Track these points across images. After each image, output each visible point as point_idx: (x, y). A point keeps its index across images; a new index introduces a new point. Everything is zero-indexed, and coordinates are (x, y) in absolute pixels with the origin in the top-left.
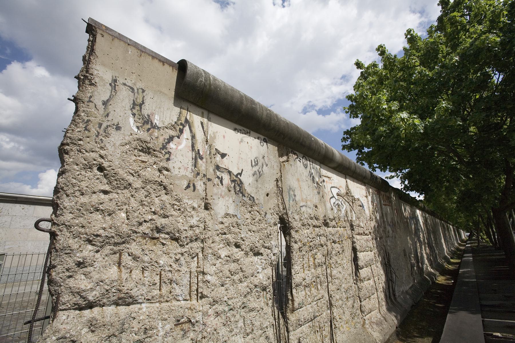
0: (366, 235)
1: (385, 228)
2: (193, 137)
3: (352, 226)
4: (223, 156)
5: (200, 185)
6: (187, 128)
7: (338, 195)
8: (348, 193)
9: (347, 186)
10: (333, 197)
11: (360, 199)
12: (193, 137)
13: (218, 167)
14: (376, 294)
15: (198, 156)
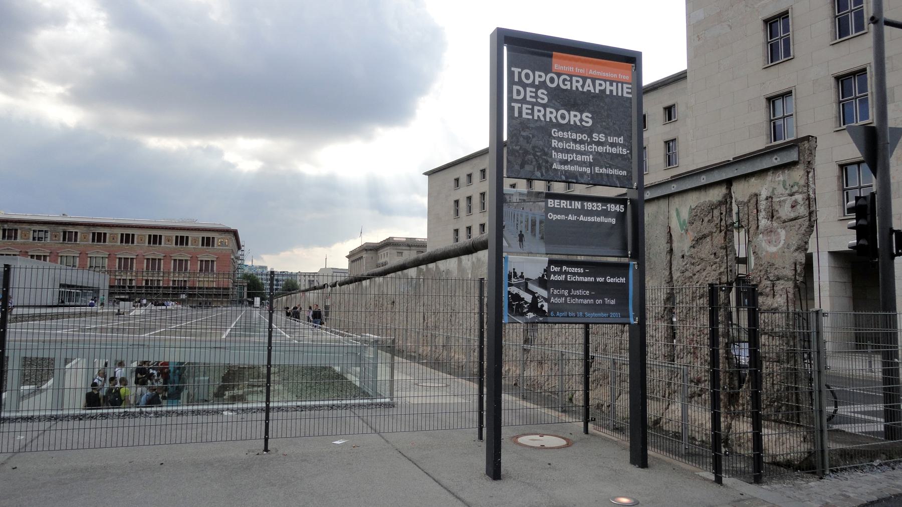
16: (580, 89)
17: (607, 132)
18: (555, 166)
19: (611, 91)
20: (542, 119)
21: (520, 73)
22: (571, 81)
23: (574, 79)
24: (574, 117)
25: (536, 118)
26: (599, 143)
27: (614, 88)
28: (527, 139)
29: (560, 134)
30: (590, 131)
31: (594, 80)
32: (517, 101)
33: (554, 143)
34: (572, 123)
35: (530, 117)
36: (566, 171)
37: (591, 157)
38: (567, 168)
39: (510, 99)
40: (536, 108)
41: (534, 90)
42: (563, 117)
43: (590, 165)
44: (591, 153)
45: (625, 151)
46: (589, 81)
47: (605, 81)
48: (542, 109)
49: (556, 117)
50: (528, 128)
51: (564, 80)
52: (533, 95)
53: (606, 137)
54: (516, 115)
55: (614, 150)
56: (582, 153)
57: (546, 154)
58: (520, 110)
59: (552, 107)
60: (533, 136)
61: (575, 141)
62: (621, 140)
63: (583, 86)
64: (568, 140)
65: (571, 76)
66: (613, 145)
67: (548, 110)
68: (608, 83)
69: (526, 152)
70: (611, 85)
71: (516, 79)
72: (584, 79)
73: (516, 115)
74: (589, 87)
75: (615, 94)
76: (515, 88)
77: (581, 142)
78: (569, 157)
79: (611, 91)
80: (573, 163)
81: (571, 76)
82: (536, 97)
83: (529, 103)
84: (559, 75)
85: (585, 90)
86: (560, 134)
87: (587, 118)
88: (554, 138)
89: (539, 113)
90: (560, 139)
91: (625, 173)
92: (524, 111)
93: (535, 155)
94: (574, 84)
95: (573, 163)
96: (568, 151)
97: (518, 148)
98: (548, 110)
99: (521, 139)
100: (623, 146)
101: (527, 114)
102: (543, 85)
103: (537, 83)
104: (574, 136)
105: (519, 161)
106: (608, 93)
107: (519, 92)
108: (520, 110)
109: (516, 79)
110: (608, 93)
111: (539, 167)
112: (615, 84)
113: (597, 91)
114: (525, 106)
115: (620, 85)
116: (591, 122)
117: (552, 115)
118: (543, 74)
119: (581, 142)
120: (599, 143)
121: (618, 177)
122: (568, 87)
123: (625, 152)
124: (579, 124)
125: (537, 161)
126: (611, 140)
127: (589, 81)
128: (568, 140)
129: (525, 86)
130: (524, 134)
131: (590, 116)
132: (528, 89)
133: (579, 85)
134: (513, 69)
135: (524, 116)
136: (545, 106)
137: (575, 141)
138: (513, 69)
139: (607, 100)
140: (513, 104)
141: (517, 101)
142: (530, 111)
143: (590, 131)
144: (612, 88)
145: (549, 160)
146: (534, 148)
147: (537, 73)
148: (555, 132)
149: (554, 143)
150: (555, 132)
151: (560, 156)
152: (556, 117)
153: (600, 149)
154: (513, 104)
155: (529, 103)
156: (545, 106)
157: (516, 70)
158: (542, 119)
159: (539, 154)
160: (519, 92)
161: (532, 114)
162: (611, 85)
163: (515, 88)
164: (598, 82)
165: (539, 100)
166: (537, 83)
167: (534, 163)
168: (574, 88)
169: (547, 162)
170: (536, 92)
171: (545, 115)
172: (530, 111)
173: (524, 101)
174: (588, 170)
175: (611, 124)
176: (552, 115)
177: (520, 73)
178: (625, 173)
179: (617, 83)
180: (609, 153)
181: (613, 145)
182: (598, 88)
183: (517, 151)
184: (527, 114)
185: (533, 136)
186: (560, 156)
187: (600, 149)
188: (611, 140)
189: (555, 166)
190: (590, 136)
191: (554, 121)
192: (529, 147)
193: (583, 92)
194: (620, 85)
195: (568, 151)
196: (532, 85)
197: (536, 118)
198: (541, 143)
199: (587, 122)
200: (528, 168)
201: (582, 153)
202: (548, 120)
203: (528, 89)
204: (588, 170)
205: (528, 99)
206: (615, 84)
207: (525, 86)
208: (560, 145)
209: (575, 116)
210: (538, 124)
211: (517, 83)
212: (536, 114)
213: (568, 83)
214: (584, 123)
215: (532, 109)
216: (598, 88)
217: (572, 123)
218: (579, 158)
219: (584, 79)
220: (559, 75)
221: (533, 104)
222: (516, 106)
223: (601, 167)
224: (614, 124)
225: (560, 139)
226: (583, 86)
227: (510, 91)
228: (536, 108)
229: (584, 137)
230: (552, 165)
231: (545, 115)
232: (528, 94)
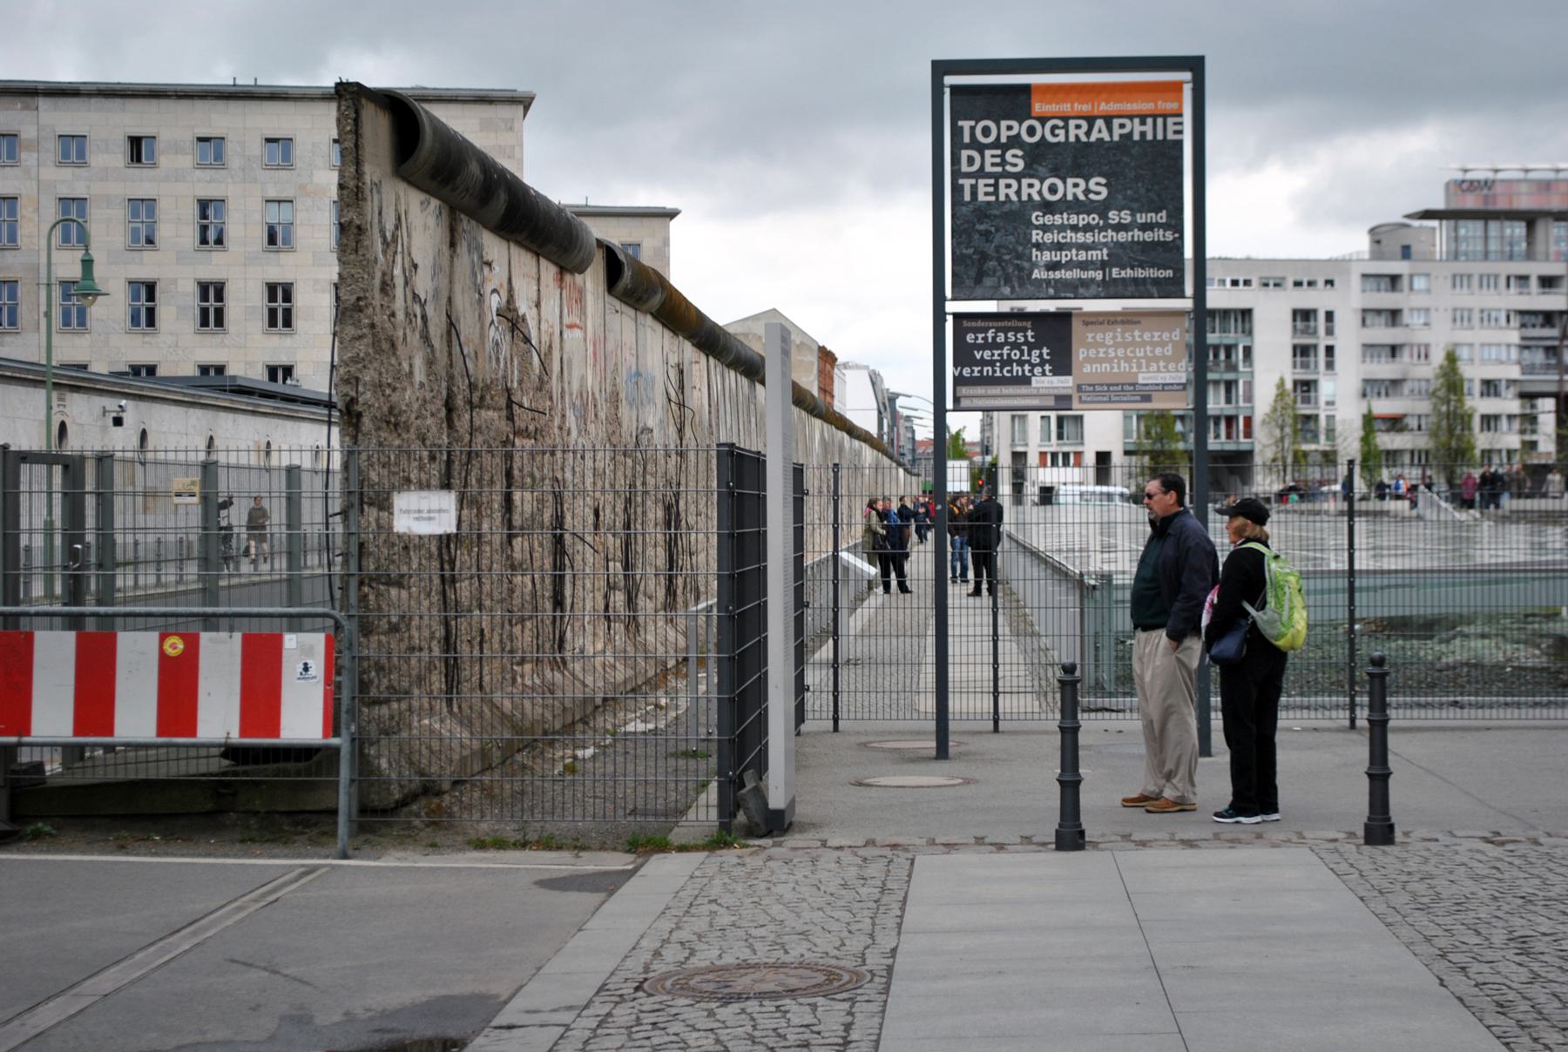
16: (1084, 139)
17: (1135, 205)
18: (1036, 274)
19: (1143, 134)
20: (1014, 198)
21: (973, 129)
22: (1066, 128)
23: (1072, 123)
24: (1072, 188)
25: (1002, 198)
26: (1119, 227)
27: (1148, 128)
28: (986, 235)
29: (1048, 220)
30: (1102, 209)
31: (1108, 119)
32: (968, 175)
33: (1036, 236)
34: (1070, 197)
35: (992, 198)
36: (1056, 281)
37: (1105, 251)
38: (1058, 275)
39: (956, 174)
40: (1002, 182)
41: (999, 152)
42: (1053, 190)
43: (1103, 265)
44: (1105, 244)
45: (1169, 236)
46: (1100, 123)
47: (1131, 117)
48: (1014, 182)
49: (1040, 193)
50: (987, 216)
51: (1054, 128)
52: (998, 160)
53: (1133, 215)
54: (967, 197)
55: (1148, 236)
56: (1086, 247)
57: (1019, 256)
58: (974, 189)
59: (1031, 176)
60: (997, 230)
61: (1075, 228)
62: (1162, 217)
63: (1088, 134)
64: (1062, 228)
65: (1065, 119)
66: (1145, 227)
67: (1025, 182)
68: (1137, 121)
70: (1143, 123)
71: (967, 139)
72: (1091, 120)
73: (967, 197)
74: (1100, 132)
75: (1150, 137)
76: (965, 154)
77: (1088, 228)
78: (1064, 257)
79: (1143, 134)
80: (1070, 265)
81: (1065, 119)
82: (1003, 163)
83: (989, 175)
84: (1043, 120)
85: (1093, 138)
86: (1048, 220)
87: (1098, 188)
88: (1037, 227)
89: (1007, 190)
90: (1045, 228)
91: (1169, 273)
92: (981, 190)
93: (999, 260)
94: (1072, 132)
95: (1070, 265)
96: (1059, 247)
97: (971, 251)
98: (1025, 182)
99: (976, 236)
100: (1165, 227)
101: (986, 194)
102: (1015, 141)
103: (1003, 140)
104: (1074, 220)
105: (973, 272)
106: (1136, 137)
107: (971, 160)
108: (974, 189)
109: (967, 139)
110: (1136, 137)
111: (1008, 280)
112: (1150, 121)
113: (1116, 138)
114: (982, 182)
115: (1160, 121)
116: (1104, 192)
117: (1034, 189)
118: (1014, 124)
119: (1088, 228)
120: (1119, 227)
122: (1062, 138)
123: (1169, 236)
124: (1082, 197)
125: (1003, 269)
126: (1141, 218)
127: (1100, 123)
128: (1062, 228)
130: (982, 227)
131: (1103, 181)
132: (988, 153)
133: (1081, 133)
134: (960, 123)
135: (981, 198)
136: (1018, 177)
137: (1075, 228)
138: (960, 123)
139: (1134, 151)
140: (961, 181)
141: (968, 175)
142: (991, 189)
143: (1102, 209)
144: (1143, 128)
145: (1026, 265)
146: (997, 249)
147: (1004, 124)
148: (1036, 217)
149: (1036, 236)
150: (1036, 217)
151: (1047, 256)
152: (1040, 193)
153: (1122, 237)
154: (961, 181)
155: (989, 175)
156: (1018, 177)
157: (966, 125)
158: (1014, 198)
159: (1007, 257)
160: (971, 160)
161: (996, 193)
162: (1143, 123)
163: (965, 154)
164: (1116, 122)
165: (1008, 168)
166: (1003, 140)
167: (999, 273)
168: (1072, 139)
169: (1020, 269)
170: (1002, 156)
171: (1018, 193)
172: (991, 189)
173: (981, 173)
174: (1099, 275)
175: (1142, 191)
176: (1034, 189)
177: (973, 129)
178: (1169, 273)
179: (1155, 117)
180: (1138, 243)
181: (1145, 227)
182: (1117, 132)
183: (970, 257)
184: (986, 194)
185: (997, 230)
186: (1047, 256)
187: (1122, 237)
188: (1141, 218)
189: (1036, 274)
190: (1103, 216)
191: (1036, 197)
193: (1088, 144)
194: (1160, 121)
195: (1059, 247)
196: (997, 144)
197: (1002, 198)
198: (1012, 239)
199: (1098, 193)
201: (1086, 247)
202: (1024, 198)
203: (988, 153)
204: (1099, 275)
205: (988, 169)
206: (1150, 121)
207: (981, 148)
208: (1048, 238)
209: (1076, 185)
210: (1007, 208)
211: (967, 147)
212: (1002, 191)
213: (1061, 132)
214: (1092, 196)
215: (996, 186)
216: (1117, 132)
217: (1070, 197)
218: (1082, 256)
219: (1091, 120)
220: (1043, 120)
221: (997, 177)
222: (967, 183)
223: (1123, 268)
224: (1148, 190)
225: (1045, 228)
226: (1088, 134)
227: (955, 160)
228: (1002, 182)
229: (1094, 219)
230: (1031, 273)
231: (1018, 193)
232: (989, 160)
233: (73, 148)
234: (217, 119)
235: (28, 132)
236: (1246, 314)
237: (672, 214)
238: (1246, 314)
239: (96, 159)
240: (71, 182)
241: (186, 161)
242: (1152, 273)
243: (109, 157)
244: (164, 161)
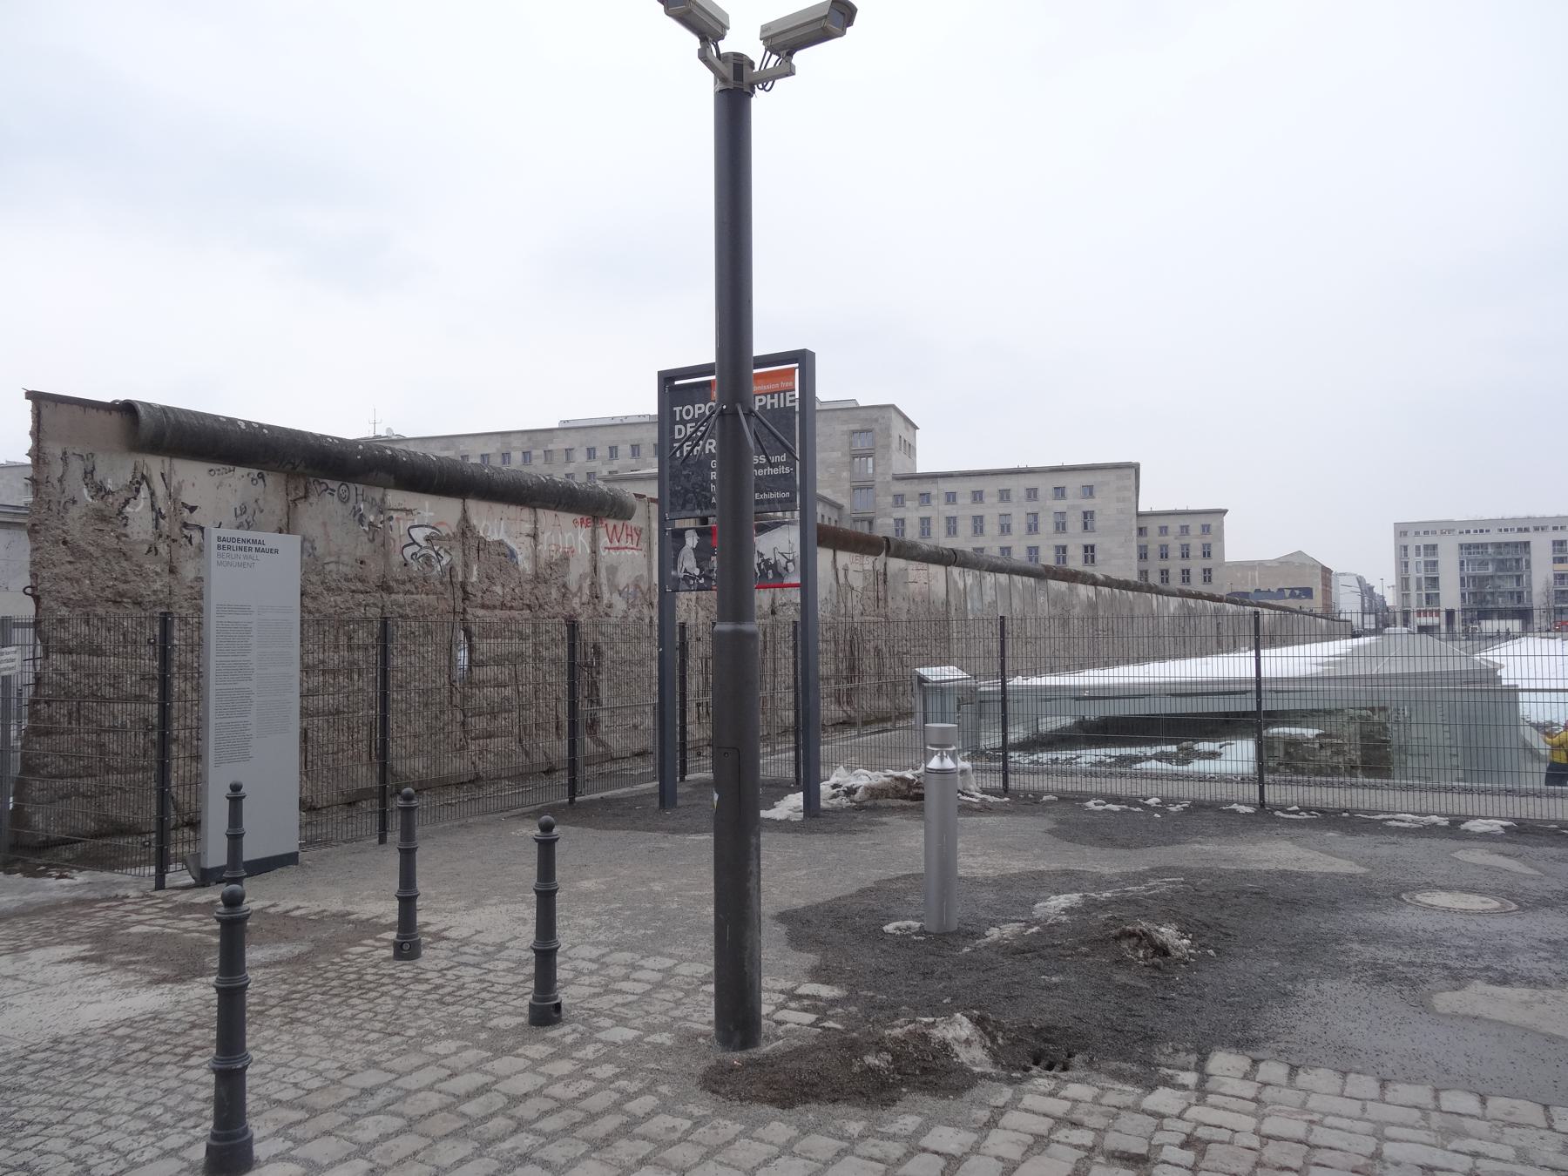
0: (511, 608)
1: (596, 597)
2: (152, 494)
3: (465, 592)
4: (192, 509)
5: (163, 548)
6: (144, 485)
7: (428, 539)
8: (466, 528)
9: (465, 518)
10: (414, 542)
11: (508, 541)
12: (152, 494)
13: (185, 525)
14: (515, 715)
15: (159, 515)
28: (687, 477)
55: (775, 471)
66: (773, 466)
69: (687, 491)
100: (785, 464)
121: (780, 501)
129: (684, 422)
157: (677, 409)
192: (689, 486)
200: (689, 506)
207: (684, 422)
233: (951, 498)
234: (1006, 483)
235: (934, 492)
236: (1527, 544)
237: (1224, 512)
238: (1527, 544)
239: (960, 501)
240: (950, 510)
241: (995, 499)
242: (777, 495)
243: (964, 500)
244: (986, 500)
